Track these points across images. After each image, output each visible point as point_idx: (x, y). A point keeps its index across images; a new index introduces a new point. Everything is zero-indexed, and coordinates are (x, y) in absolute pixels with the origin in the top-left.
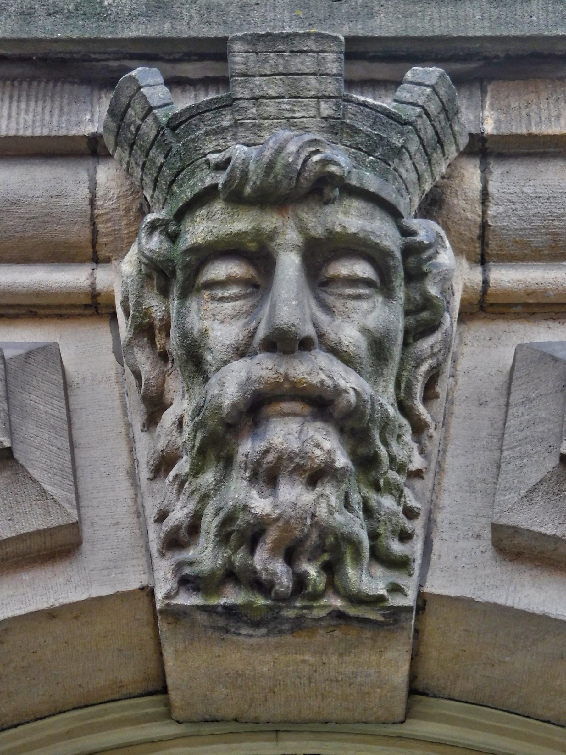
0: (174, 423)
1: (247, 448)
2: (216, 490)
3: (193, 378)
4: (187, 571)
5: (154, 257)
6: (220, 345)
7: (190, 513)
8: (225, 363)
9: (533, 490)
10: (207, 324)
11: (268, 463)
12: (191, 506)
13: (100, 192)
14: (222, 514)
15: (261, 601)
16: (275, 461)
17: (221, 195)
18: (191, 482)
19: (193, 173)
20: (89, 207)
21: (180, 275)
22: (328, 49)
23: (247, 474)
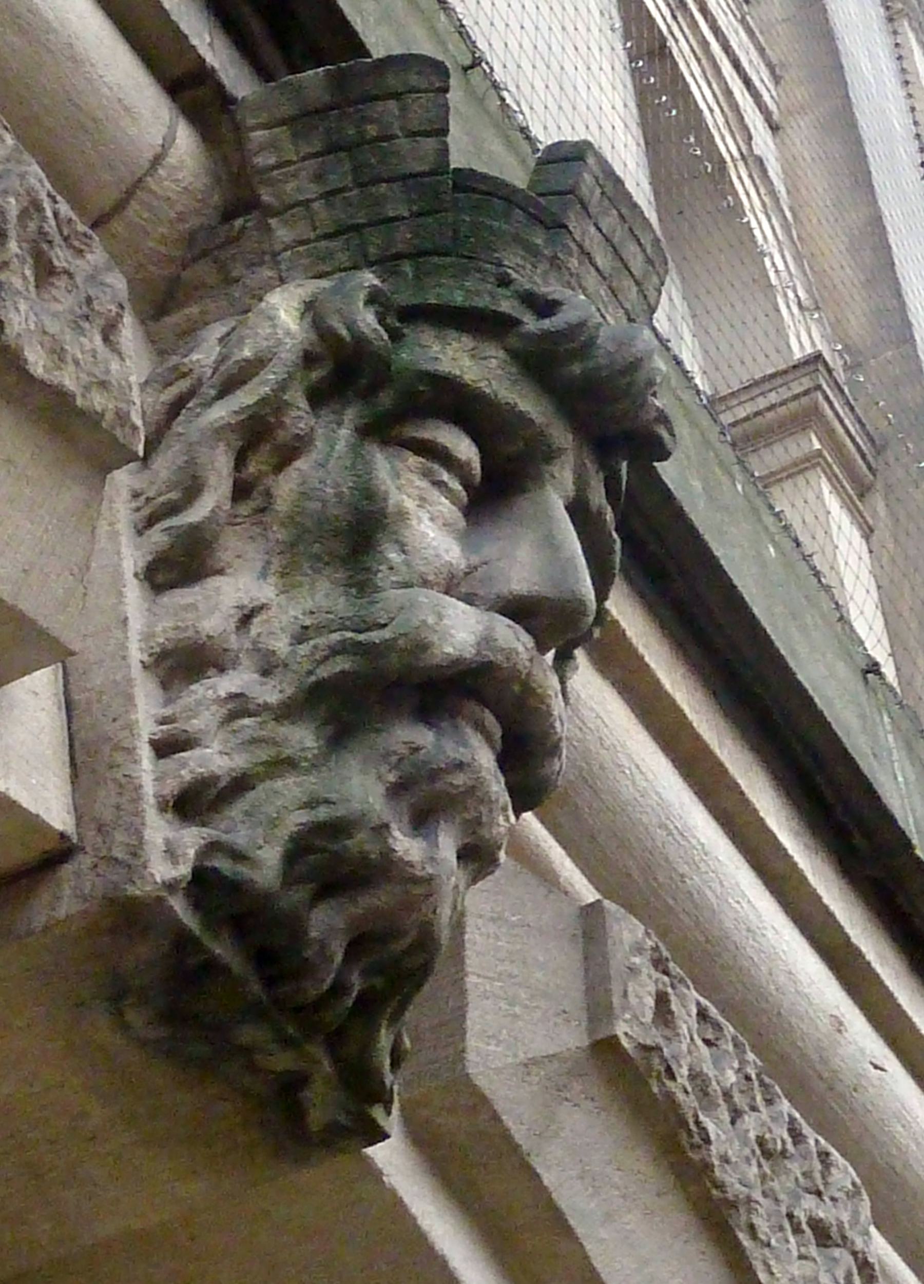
0: (240, 607)
1: (411, 736)
2: (314, 765)
3: (327, 564)
4: (223, 864)
5: (376, 343)
6: (432, 552)
7: (233, 770)
8: (425, 583)
9: (534, 1062)
10: (410, 504)
11: (451, 784)
12: (240, 762)
13: (171, 160)
14: (323, 813)
15: (256, 988)
16: (461, 789)
17: (513, 341)
18: (264, 722)
19: (466, 272)
20: (147, 165)
21: (386, 399)
22: (657, 265)
23: (392, 778)
